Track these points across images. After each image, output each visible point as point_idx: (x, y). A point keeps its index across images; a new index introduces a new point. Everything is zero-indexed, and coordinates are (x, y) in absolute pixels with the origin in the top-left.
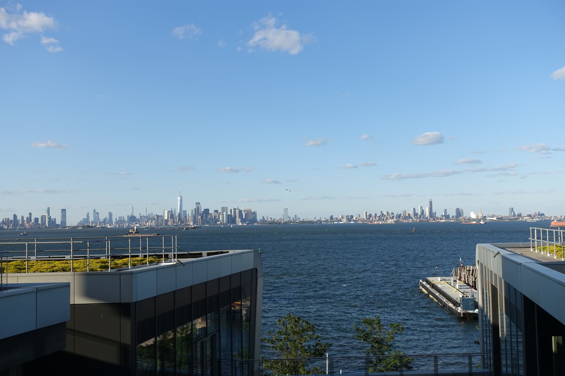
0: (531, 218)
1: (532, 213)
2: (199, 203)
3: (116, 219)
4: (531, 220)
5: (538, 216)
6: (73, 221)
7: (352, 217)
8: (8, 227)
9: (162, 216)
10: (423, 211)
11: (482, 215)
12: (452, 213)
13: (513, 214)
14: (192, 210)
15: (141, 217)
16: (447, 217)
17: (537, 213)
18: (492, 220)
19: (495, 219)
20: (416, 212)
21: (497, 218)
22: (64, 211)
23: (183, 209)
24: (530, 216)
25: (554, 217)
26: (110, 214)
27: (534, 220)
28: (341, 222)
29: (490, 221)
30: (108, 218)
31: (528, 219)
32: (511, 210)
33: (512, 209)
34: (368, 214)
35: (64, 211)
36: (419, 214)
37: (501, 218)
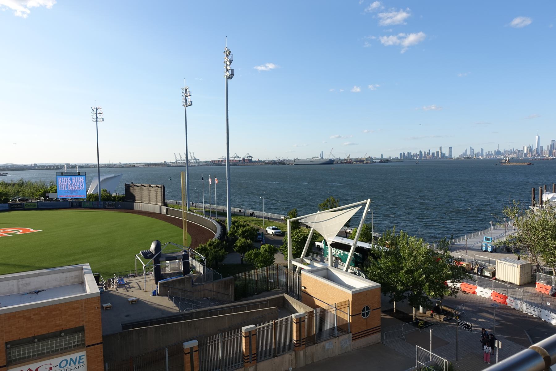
2: (555, 141)
3: (486, 153)
6: (456, 154)
8: (417, 158)
9: (522, 150)
14: (548, 146)
15: (505, 151)
22: (450, 148)
23: (541, 145)
26: (482, 150)
30: (480, 153)
35: (450, 148)
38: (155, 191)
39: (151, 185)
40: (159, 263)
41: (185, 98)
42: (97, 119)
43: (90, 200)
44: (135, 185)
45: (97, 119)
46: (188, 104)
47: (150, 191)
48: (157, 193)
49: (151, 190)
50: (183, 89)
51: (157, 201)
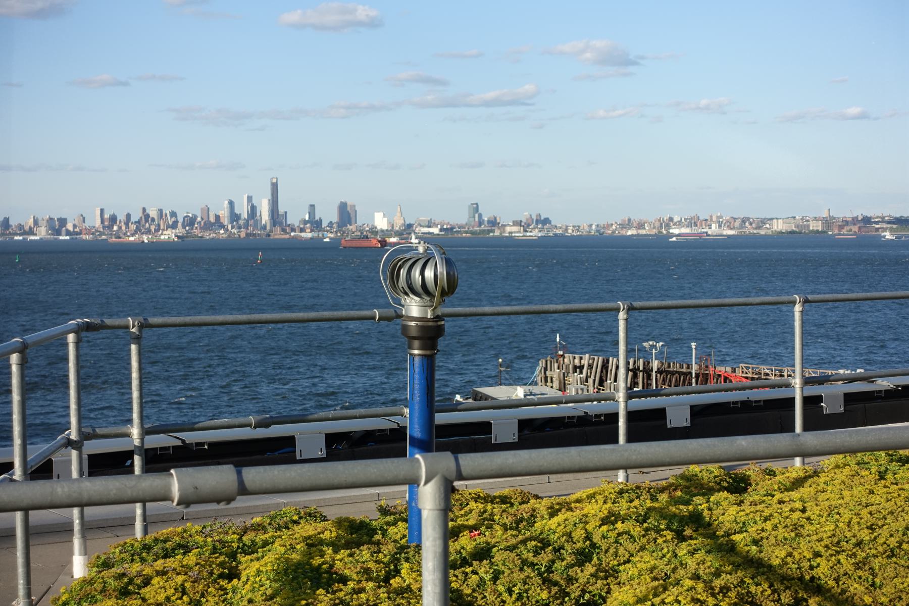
0: (522, 228)
1: (524, 216)
4: (521, 235)
5: (537, 224)
7: (63, 222)
10: (253, 210)
11: (403, 222)
12: (329, 215)
13: (477, 219)
16: (316, 225)
17: (534, 218)
18: (429, 233)
19: (436, 230)
20: (237, 211)
21: (441, 230)
24: (518, 223)
25: (574, 227)
27: (528, 234)
28: (33, 238)
29: (425, 235)
31: (515, 232)
32: (474, 208)
33: (475, 206)
34: (106, 216)
36: (242, 217)
37: (452, 228)
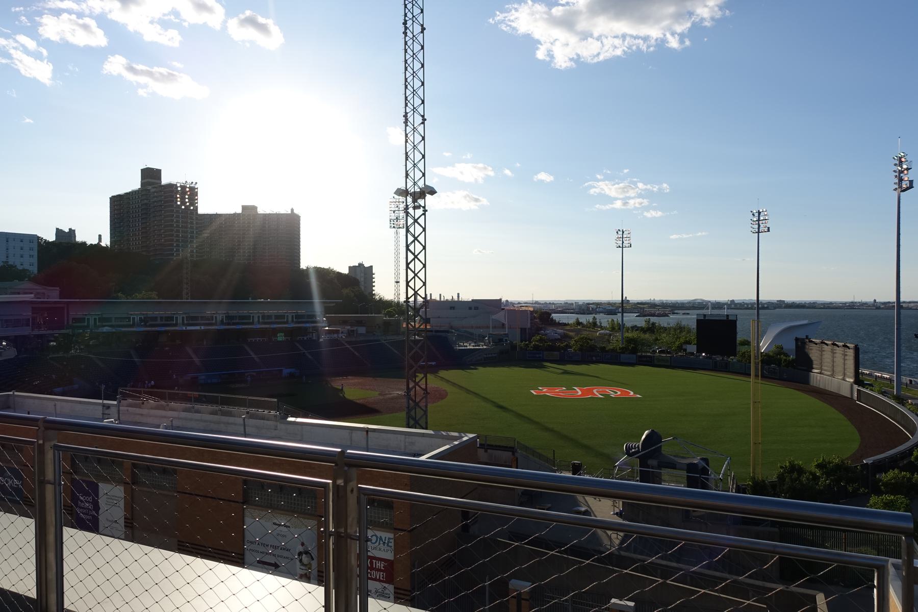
38: (843, 354)
39: (837, 343)
40: (687, 475)
41: (899, 175)
42: (759, 228)
43: (742, 361)
44: (812, 341)
45: (759, 228)
46: (903, 186)
47: (835, 353)
48: (846, 359)
49: (837, 351)
50: (896, 158)
51: (844, 374)
